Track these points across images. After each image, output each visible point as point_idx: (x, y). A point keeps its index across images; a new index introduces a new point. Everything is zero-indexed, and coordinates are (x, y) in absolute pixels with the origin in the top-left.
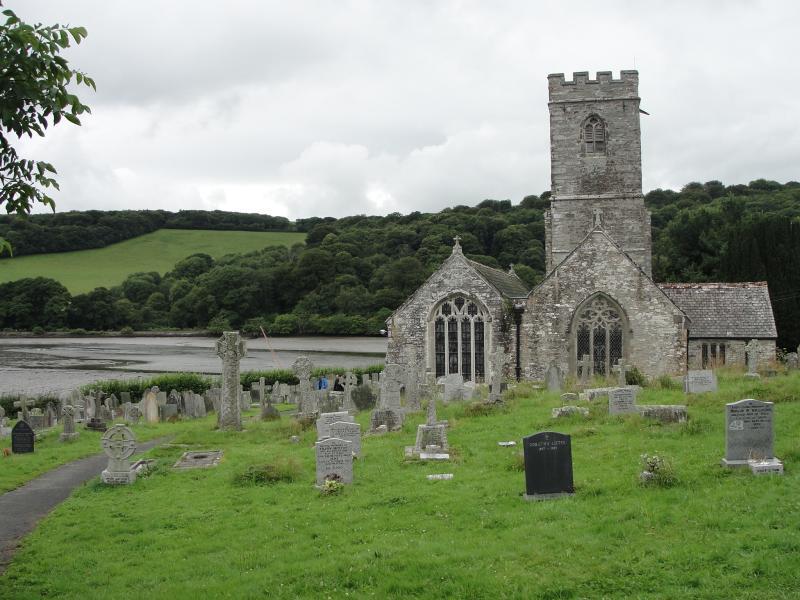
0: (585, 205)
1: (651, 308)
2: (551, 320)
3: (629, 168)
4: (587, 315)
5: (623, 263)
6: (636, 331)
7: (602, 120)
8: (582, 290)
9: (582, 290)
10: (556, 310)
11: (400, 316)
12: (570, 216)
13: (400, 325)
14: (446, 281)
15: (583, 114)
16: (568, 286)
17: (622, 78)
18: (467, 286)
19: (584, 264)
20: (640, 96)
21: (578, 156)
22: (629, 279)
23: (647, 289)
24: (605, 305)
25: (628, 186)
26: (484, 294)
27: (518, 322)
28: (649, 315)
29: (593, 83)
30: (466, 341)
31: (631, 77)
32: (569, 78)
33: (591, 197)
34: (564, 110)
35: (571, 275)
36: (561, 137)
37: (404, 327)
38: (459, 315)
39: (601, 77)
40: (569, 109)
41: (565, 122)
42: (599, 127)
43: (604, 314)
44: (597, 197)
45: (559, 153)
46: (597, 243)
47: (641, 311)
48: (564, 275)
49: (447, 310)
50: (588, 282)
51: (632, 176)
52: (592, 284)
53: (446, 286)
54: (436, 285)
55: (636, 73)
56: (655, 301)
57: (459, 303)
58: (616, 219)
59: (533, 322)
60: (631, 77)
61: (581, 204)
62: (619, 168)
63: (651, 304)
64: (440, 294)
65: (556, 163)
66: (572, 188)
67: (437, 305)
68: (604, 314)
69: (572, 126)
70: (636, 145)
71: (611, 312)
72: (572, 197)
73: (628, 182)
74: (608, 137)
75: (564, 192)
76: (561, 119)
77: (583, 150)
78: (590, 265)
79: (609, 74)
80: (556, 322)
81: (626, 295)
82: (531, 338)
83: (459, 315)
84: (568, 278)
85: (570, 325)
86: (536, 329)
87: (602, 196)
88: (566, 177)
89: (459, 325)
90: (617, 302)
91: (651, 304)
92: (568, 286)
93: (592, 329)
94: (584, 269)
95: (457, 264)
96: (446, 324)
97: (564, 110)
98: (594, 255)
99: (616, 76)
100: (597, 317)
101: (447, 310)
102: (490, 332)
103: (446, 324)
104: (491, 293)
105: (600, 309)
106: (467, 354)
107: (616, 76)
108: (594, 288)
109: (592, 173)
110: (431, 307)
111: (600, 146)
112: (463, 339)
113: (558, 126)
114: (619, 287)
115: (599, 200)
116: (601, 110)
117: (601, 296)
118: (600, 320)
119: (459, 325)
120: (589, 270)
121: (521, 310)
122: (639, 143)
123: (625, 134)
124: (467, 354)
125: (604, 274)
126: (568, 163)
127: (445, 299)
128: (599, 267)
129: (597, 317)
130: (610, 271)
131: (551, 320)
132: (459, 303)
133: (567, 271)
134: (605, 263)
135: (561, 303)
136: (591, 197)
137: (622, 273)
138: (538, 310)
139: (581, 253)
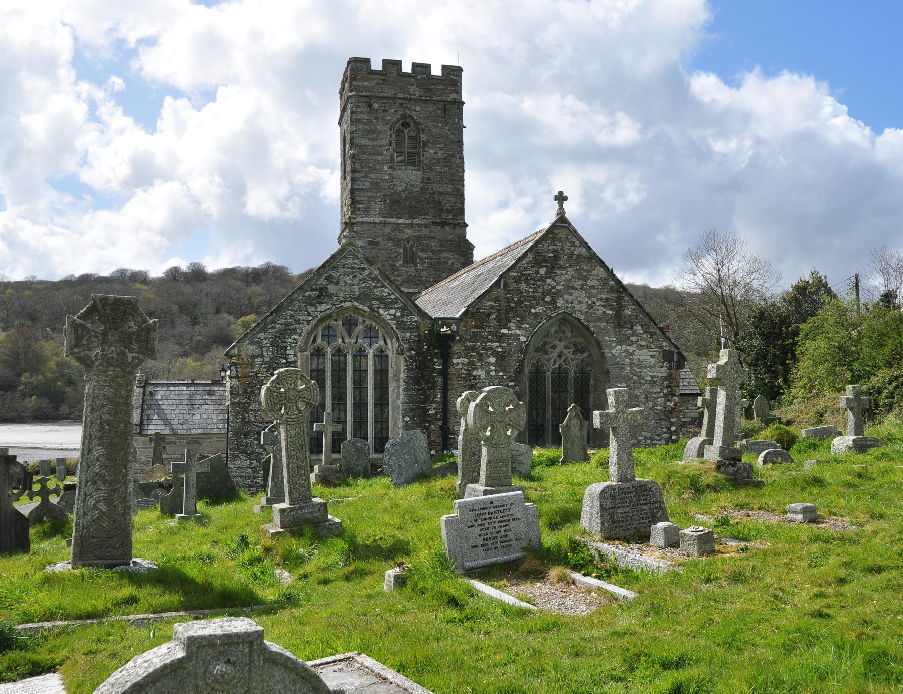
0: (393, 231)
1: (633, 339)
2: (495, 353)
4: (542, 349)
5: (595, 273)
6: (614, 371)
7: (417, 124)
8: (539, 309)
9: (539, 309)
10: (501, 338)
11: (252, 343)
12: (373, 244)
13: (253, 357)
14: (331, 288)
16: (519, 303)
18: (365, 297)
19: (542, 271)
21: (386, 168)
22: (604, 296)
23: (627, 311)
24: (569, 334)
25: (449, 211)
26: (393, 311)
27: (446, 357)
28: (630, 349)
30: (359, 384)
31: (453, 74)
32: (377, 65)
33: (401, 221)
34: (370, 106)
35: (523, 286)
36: (364, 142)
37: (258, 361)
38: (347, 343)
39: (418, 69)
40: (376, 106)
41: (370, 122)
42: (412, 134)
43: (566, 347)
44: (408, 221)
45: (361, 161)
46: (560, 241)
47: (620, 342)
48: (513, 286)
49: (329, 335)
50: (548, 299)
51: (453, 199)
52: (554, 301)
53: (331, 295)
54: (313, 294)
55: (457, 71)
56: (639, 329)
57: (350, 324)
58: (432, 251)
59: (467, 356)
60: (453, 74)
61: (388, 230)
62: (437, 187)
63: (634, 333)
64: (322, 307)
65: (356, 174)
66: (377, 207)
67: (314, 328)
68: (566, 347)
69: (379, 128)
70: (458, 161)
71: (576, 345)
72: (378, 219)
75: (367, 212)
76: (365, 117)
77: (392, 160)
78: (551, 273)
79: (427, 67)
80: (501, 358)
81: (600, 319)
82: (465, 380)
83: (347, 343)
84: (519, 291)
85: (522, 362)
86: (472, 366)
87: (415, 221)
88: (369, 194)
89: (349, 359)
90: (587, 328)
91: (634, 333)
92: (519, 303)
93: (550, 369)
94: (543, 279)
95: (350, 262)
96: (329, 355)
97: (370, 106)
98: (557, 258)
99: (436, 71)
100: (557, 351)
101: (329, 335)
102: (398, 367)
103: (329, 355)
104: (403, 309)
105: (560, 340)
106: (360, 406)
107: (436, 71)
108: (556, 308)
109: (404, 191)
110: (306, 328)
111: (413, 160)
112: (354, 382)
113: (361, 126)
114: (590, 307)
115: (412, 226)
116: (417, 111)
117: (567, 320)
118: (560, 356)
119: (349, 359)
120: (548, 280)
121: (451, 338)
122: (462, 158)
123: (446, 145)
124: (360, 406)
125: (570, 288)
126: (373, 175)
127: (329, 316)
128: (565, 275)
129: (557, 351)
130: (578, 283)
131: (495, 353)
132: (350, 324)
133: (517, 280)
134: (571, 271)
135: (509, 329)
136: (401, 221)
137: (593, 287)
138: (476, 337)
139: (539, 254)
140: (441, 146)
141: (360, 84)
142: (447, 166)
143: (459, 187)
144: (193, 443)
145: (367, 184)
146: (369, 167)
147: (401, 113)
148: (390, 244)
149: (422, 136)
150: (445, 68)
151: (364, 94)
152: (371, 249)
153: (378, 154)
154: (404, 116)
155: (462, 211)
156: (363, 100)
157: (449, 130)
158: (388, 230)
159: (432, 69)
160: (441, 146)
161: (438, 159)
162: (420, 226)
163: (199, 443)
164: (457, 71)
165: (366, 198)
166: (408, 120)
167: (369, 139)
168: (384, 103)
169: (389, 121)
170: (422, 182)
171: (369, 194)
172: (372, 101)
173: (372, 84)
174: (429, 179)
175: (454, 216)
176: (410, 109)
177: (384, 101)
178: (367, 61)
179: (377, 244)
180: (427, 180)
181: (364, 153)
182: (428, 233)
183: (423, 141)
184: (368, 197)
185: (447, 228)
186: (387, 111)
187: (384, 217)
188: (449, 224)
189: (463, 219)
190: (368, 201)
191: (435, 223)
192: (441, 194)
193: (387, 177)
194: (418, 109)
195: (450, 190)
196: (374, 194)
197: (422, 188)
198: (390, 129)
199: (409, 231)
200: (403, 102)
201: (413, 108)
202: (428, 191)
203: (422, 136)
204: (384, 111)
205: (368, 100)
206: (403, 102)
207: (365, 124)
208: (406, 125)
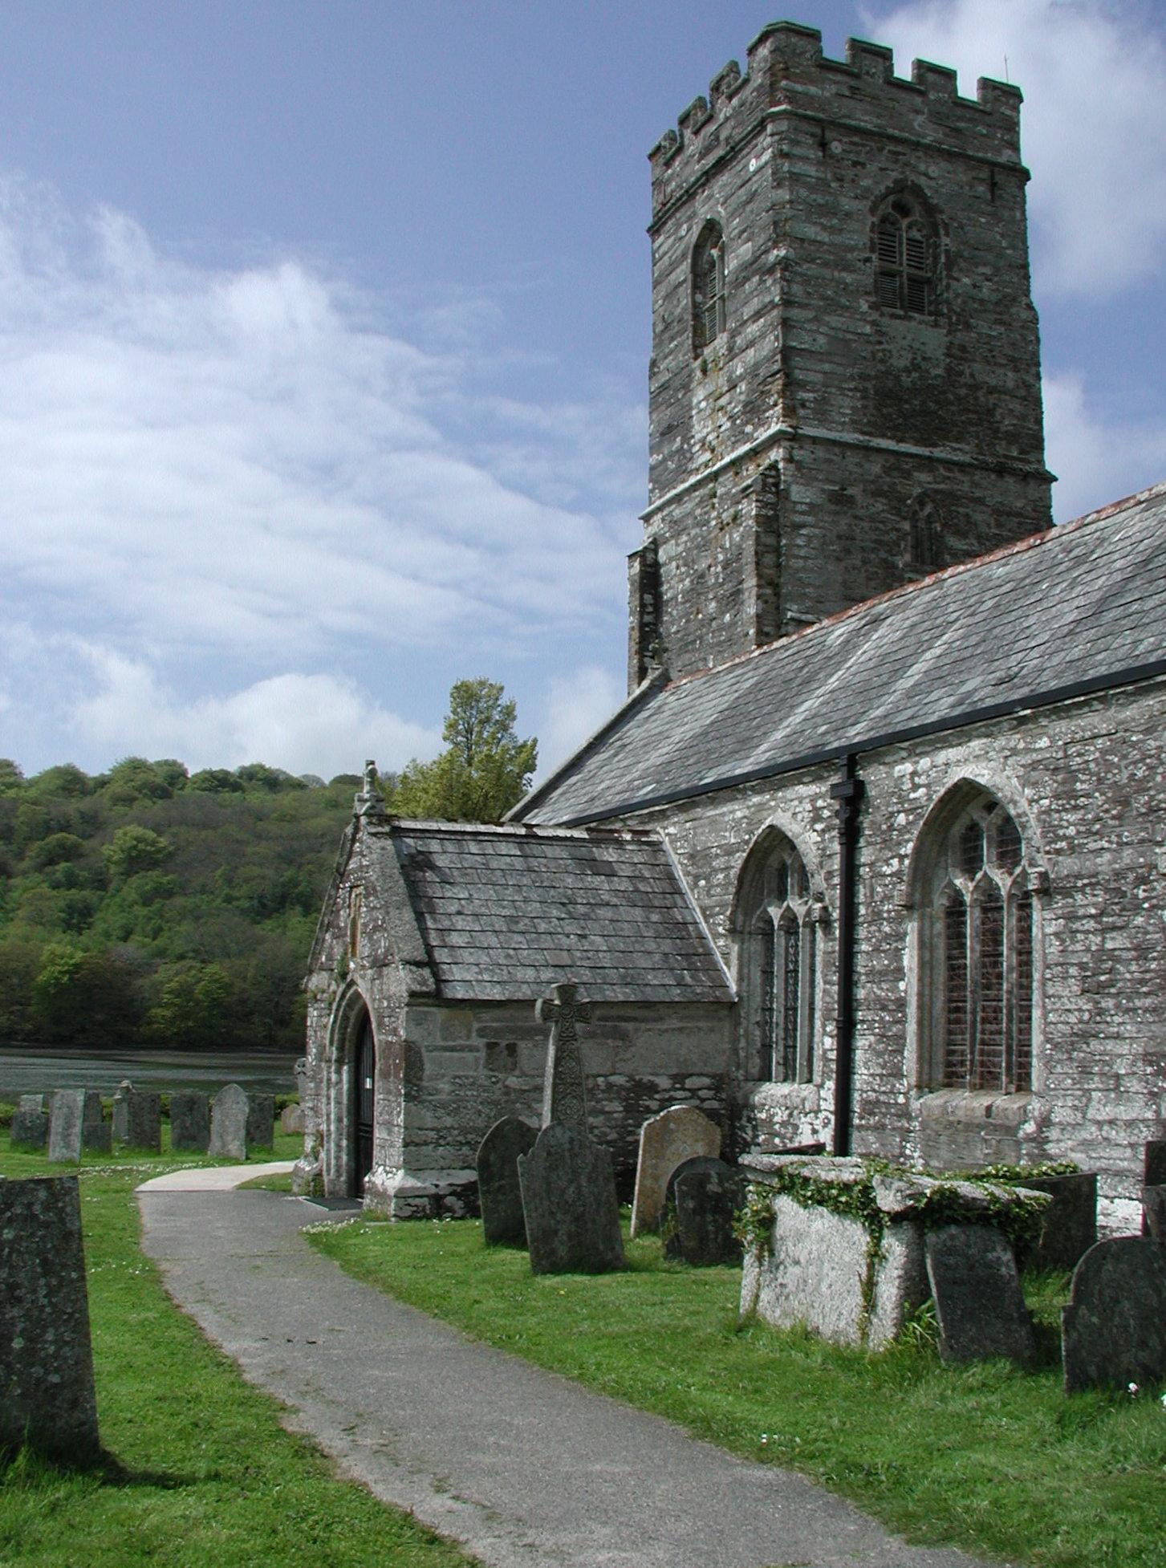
0: (887, 470)
3: (1010, 379)
7: (931, 210)
12: (840, 499)
15: (877, 176)
17: (984, 99)
20: (1026, 161)
29: (901, 85)
32: (836, 51)
33: (904, 447)
34: (823, 145)
36: (811, 231)
39: (931, 77)
40: (836, 147)
41: (821, 185)
44: (924, 451)
45: (807, 280)
51: (1016, 406)
55: (1012, 95)
58: (979, 537)
61: (875, 468)
65: (795, 313)
66: (845, 405)
69: (847, 204)
73: (1008, 423)
74: (949, 265)
76: (812, 171)
87: (938, 453)
88: (827, 367)
97: (823, 145)
109: (907, 371)
113: (803, 193)
115: (928, 463)
123: (997, 271)
126: (835, 320)
136: (904, 447)
140: (987, 270)
141: (799, 88)
142: (1002, 323)
143: (1030, 379)
144: (605, 1035)
145: (822, 340)
146: (824, 298)
147: (895, 175)
148: (879, 506)
149: (945, 240)
150: (986, 84)
151: (809, 113)
152: (837, 513)
153: (844, 269)
154: (901, 187)
155: (1037, 443)
156: (805, 126)
157: (1002, 235)
158: (875, 468)
159: (959, 83)
160: (987, 270)
161: (982, 301)
162: (949, 464)
163: (624, 1036)
164: (1012, 95)
165: (819, 377)
166: (909, 199)
167: (824, 228)
168: (855, 144)
169: (867, 190)
170: (948, 355)
171: (827, 367)
172: (829, 135)
173: (827, 94)
174: (963, 348)
175: (1022, 452)
176: (914, 169)
177: (856, 139)
178: (814, 36)
179: (851, 500)
180: (958, 353)
181: (812, 261)
182: (966, 487)
183: (947, 252)
184: (825, 373)
185: (1010, 480)
186: (863, 165)
187: (863, 433)
188: (1013, 472)
189: (1041, 461)
190: (825, 385)
191: (984, 467)
192: (992, 390)
193: (868, 329)
194: (933, 171)
195: (1011, 384)
196: (840, 370)
197: (949, 370)
198: (873, 211)
199: (924, 477)
200: (899, 149)
201: (922, 167)
202: (962, 380)
203: (945, 240)
204: (855, 164)
205: (818, 131)
206: (899, 149)
207: (812, 189)
208: (903, 210)
